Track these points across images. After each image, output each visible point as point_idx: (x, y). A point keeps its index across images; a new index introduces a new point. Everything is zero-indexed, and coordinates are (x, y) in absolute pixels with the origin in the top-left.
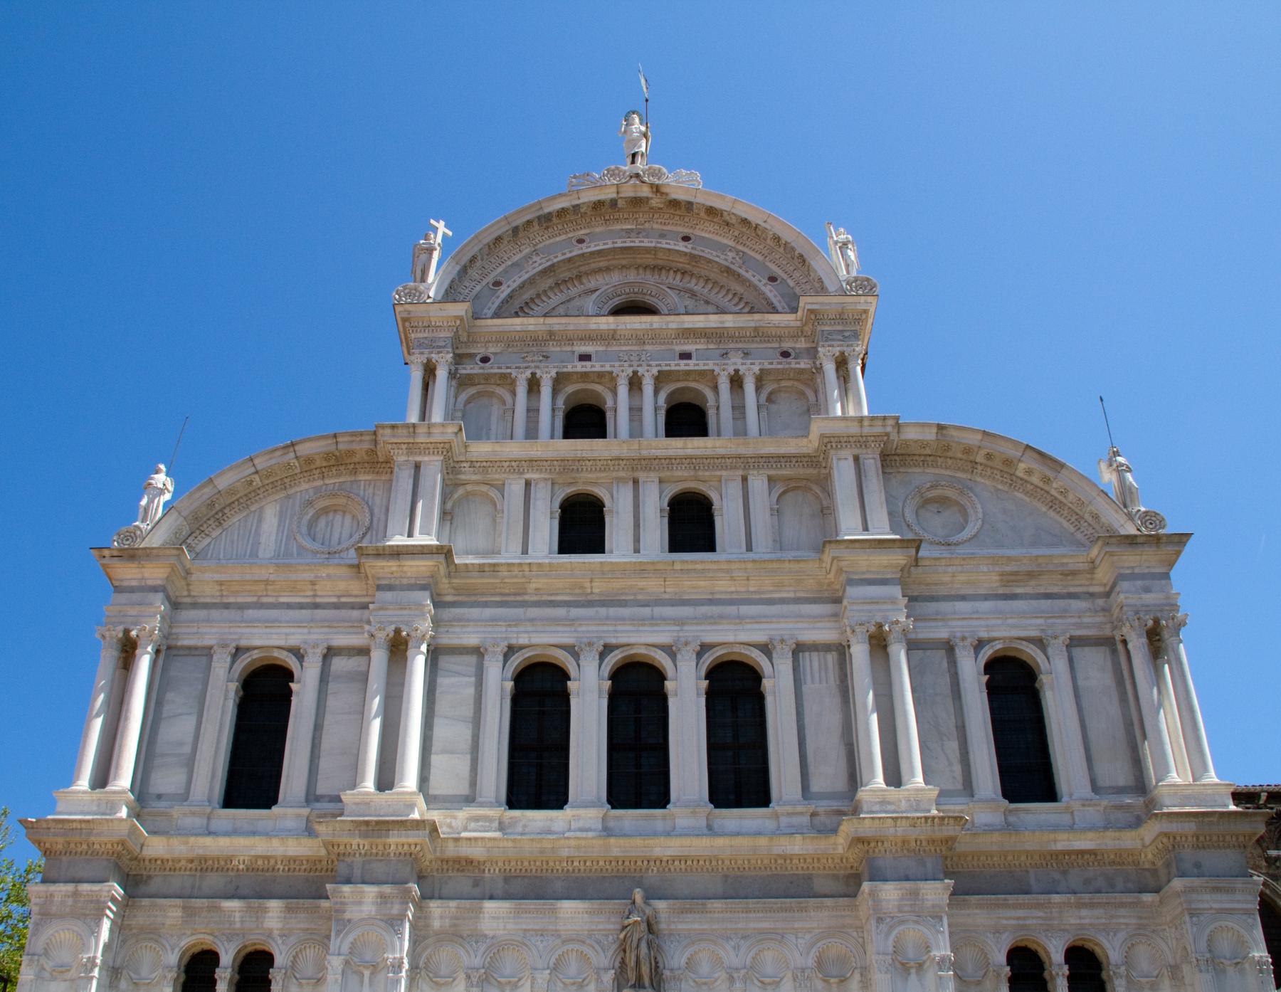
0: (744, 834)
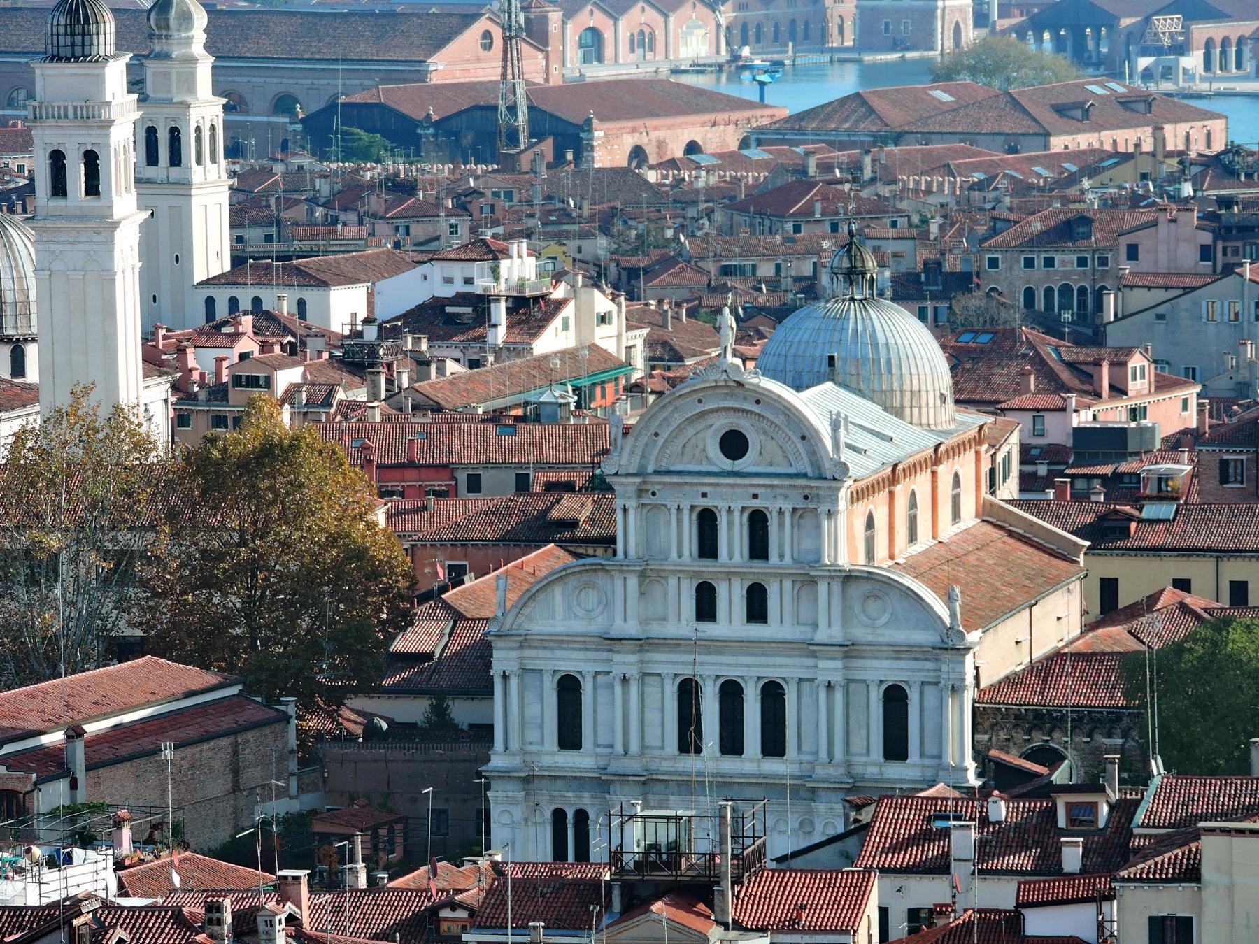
0: (773, 766)
